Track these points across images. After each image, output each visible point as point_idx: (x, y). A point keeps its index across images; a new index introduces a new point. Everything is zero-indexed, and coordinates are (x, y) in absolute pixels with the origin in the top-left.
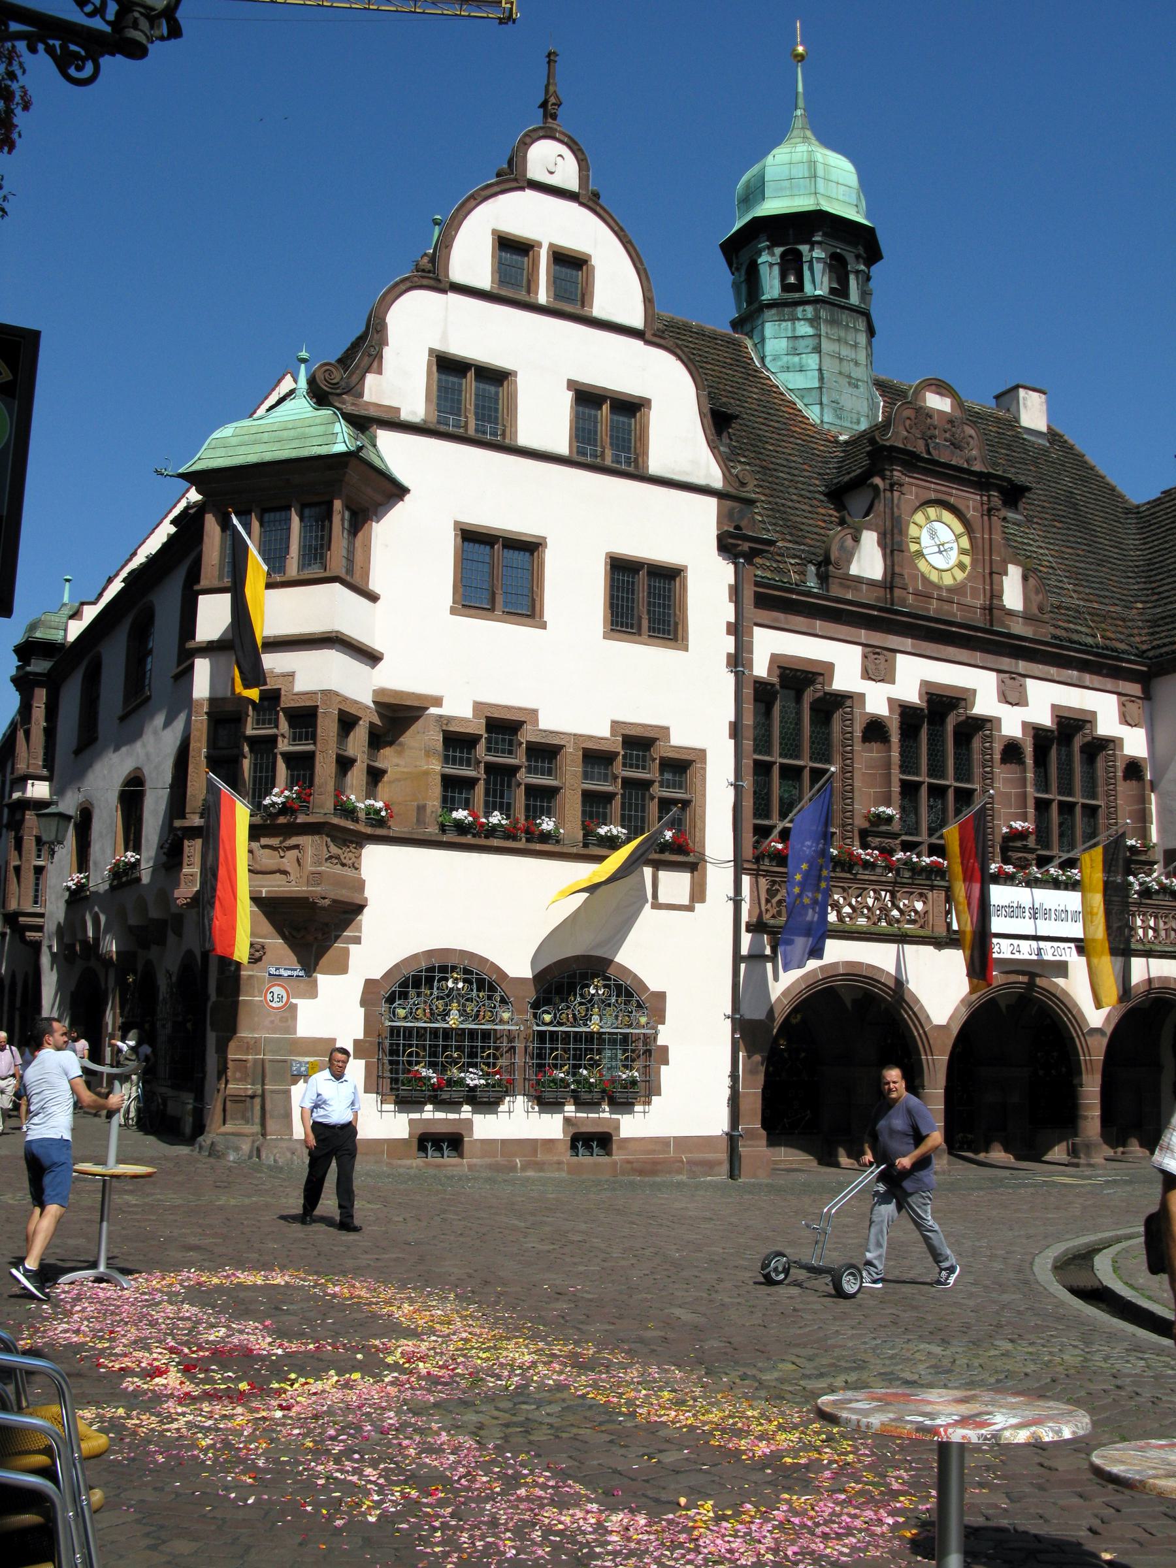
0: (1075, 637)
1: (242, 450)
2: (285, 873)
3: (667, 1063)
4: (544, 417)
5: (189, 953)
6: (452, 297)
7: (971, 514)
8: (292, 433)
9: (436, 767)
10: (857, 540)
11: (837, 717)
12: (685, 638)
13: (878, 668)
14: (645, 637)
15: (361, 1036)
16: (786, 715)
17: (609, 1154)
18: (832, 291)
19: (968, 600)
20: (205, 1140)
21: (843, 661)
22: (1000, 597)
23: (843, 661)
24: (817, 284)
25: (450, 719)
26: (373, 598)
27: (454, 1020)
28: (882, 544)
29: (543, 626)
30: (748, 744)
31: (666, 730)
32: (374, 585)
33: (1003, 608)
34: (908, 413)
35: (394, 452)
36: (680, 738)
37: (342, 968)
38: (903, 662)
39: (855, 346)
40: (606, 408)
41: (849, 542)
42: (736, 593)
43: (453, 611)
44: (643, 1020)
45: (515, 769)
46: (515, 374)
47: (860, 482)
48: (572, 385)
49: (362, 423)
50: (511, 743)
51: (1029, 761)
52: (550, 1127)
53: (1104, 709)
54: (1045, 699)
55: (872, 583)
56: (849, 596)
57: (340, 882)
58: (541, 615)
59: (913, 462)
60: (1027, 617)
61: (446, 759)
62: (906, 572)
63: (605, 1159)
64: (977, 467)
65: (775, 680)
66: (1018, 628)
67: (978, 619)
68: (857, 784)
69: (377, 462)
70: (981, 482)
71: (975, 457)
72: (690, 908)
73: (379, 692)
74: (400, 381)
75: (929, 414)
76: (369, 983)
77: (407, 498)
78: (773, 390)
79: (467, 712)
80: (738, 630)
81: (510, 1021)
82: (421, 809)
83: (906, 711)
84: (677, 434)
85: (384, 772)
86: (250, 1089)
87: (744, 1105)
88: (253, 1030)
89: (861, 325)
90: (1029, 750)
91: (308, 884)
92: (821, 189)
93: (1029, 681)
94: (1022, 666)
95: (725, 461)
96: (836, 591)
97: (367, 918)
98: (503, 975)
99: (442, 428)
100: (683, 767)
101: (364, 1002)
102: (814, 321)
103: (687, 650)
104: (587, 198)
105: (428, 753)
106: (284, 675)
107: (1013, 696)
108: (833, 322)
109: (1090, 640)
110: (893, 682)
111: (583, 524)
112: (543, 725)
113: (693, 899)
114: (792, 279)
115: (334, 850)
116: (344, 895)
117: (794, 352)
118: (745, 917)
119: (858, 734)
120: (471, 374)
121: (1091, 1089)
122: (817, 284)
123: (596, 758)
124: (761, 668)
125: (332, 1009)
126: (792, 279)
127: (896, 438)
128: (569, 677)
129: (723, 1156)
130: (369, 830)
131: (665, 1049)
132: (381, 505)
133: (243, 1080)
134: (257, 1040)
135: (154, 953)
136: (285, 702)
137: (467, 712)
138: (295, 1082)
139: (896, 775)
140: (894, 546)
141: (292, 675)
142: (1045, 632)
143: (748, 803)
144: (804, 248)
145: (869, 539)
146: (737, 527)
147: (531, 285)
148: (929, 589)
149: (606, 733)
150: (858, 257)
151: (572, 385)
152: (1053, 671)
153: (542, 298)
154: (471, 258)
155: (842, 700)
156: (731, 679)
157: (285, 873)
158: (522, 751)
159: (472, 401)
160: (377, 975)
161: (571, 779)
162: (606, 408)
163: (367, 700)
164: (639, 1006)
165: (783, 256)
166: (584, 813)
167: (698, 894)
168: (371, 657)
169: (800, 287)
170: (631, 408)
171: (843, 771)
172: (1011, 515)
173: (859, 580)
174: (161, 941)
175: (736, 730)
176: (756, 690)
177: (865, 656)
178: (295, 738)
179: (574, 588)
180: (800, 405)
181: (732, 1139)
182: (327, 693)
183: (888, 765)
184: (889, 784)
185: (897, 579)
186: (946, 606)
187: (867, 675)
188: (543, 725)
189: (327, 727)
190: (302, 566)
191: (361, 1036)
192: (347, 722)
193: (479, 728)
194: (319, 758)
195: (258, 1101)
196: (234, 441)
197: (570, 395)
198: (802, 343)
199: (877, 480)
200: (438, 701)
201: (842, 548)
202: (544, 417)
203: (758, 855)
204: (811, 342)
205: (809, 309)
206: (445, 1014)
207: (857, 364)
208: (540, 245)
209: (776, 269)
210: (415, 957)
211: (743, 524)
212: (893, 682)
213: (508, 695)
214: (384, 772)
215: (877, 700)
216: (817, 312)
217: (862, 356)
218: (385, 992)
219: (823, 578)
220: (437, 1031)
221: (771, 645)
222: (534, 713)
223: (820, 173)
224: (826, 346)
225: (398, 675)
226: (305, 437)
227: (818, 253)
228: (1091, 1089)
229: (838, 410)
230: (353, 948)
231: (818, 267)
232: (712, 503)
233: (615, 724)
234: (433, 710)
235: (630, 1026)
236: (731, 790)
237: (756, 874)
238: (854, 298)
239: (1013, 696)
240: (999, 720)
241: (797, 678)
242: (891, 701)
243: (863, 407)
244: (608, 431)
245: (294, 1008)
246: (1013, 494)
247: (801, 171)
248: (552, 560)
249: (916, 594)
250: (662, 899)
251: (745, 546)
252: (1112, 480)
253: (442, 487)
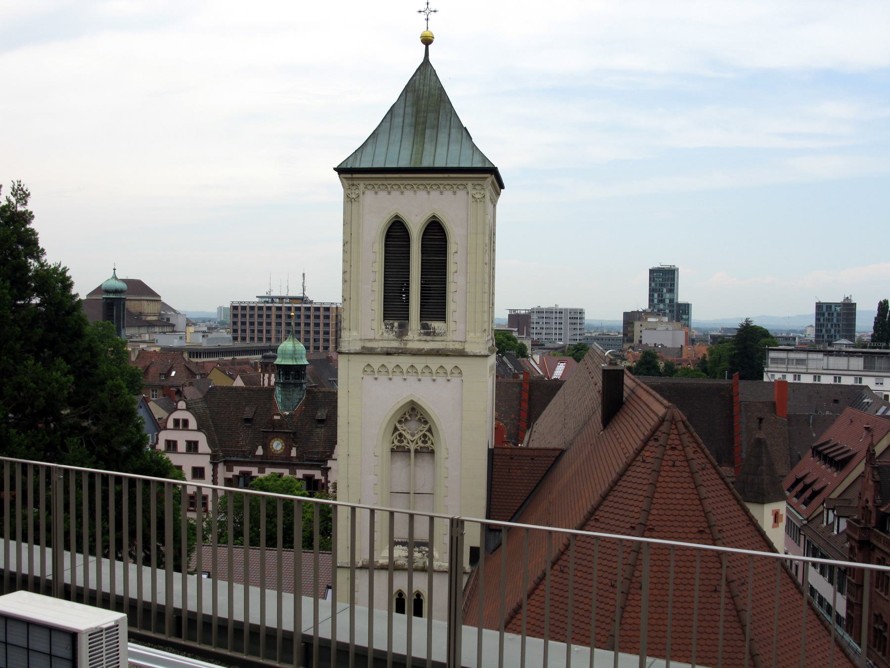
4: (182, 447)
13: (262, 471)
60: (297, 457)
104: (188, 409)
140: (266, 447)
145: (260, 448)
154: (170, 424)
155: (255, 477)
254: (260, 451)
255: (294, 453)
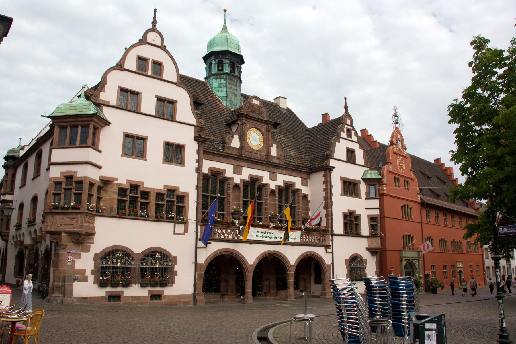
0: (290, 163)
1: (66, 111)
2: (73, 225)
3: (177, 275)
4: (149, 105)
5: (48, 245)
6: (125, 72)
7: (263, 131)
8: (79, 107)
9: (116, 197)
10: (233, 137)
11: (226, 183)
12: (184, 164)
13: (237, 171)
14: (174, 163)
15: (93, 269)
16: (212, 185)
17: (161, 300)
18: (231, 71)
19: (262, 153)
20: (48, 298)
21: (228, 169)
22: (270, 153)
23: (228, 169)
24: (227, 69)
25: (120, 184)
26: (100, 152)
27: (119, 265)
28: (240, 139)
29: (146, 160)
30: (201, 191)
31: (179, 187)
32: (100, 149)
33: (271, 155)
34: (248, 105)
35: (107, 113)
36: (183, 190)
37: (88, 250)
38: (244, 169)
39: (236, 86)
40: (165, 102)
41: (231, 138)
42: (198, 152)
43: (122, 156)
44: (170, 264)
45: (137, 197)
46: (141, 93)
47: (234, 123)
48: (156, 96)
49: (99, 105)
50: (137, 191)
51: (277, 195)
52: (144, 292)
53: (297, 181)
54: (281, 179)
55: (236, 149)
56: (230, 152)
57: (88, 228)
58: (146, 157)
59: (248, 117)
60: (278, 158)
61: (119, 195)
62: (246, 146)
63: (159, 301)
64: (265, 119)
65: (210, 174)
66: (275, 161)
67: (264, 158)
68: (231, 201)
69: (102, 116)
70: (267, 123)
71: (265, 116)
72: (184, 234)
73: (100, 177)
74: (110, 95)
75: (253, 105)
76: (96, 255)
77: (110, 125)
78: (214, 97)
79: (125, 182)
80: (199, 161)
81: (135, 264)
82: (112, 208)
83: (245, 182)
84: (185, 110)
85: (102, 198)
86: (61, 284)
87: (198, 286)
88: (62, 268)
89: (238, 80)
90: (277, 192)
91: (79, 228)
92: (229, 45)
93: (278, 175)
94: (276, 170)
95: (197, 116)
96: (227, 151)
97: (96, 237)
98: (133, 252)
99: (121, 107)
100: (182, 198)
101: (94, 260)
102: (225, 79)
103: (184, 166)
105: (114, 193)
106: (74, 172)
107: (273, 178)
108: (230, 80)
109: (294, 164)
110: (241, 174)
111: (158, 134)
112: (145, 186)
113: (184, 232)
114: (220, 68)
115: (87, 219)
116: (89, 231)
117: (220, 87)
118: (199, 237)
119: (232, 188)
120: (129, 93)
121: (291, 280)
122: (227, 69)
123: (159, 195)
124: (205, 170)
125: (86, 262)
126: (220, 68)
127: (243, 111)
128: (154, 174)
129: (192, 300)
130: (96, 214)
131: (177, 271)
132: (103, 127)
133: (59, 281)
134: (64, 270)
135: (39, 245)
136: (74, 179)
137: (125, 182)
138: (74, 282)
139: (242, 199)
140: (243, 138)
141: (77, 172)
142: (282, 162)
143: (200, 207)
144: (224, 60)
145: (236, 137)
146: (199, 135)
147: (146, 70)
148: (252, 151)
149: (162, 188)
150: (238, 63)
151: (157, 96)
152: (284, 171)
153: (149, 73)
156: (196, 174)
157: (73, 225)
158: (139, 193)
159: (129, 99)
160: (98, 252)
161: (152, 201)
162: (165, 102)
163: (97, 179)
164: (170, 260)
165: (218, 61)
166: (156, 209)
167: (186, 230)
168: (100, 167)
169: (222, 70)
170: (173, 103)
171: (228, 197)
172: (275, 130)
173: (233, 148)
174: (41, 242)
175: (197, 188)
176: (203, 176)
177: (234, 168)
178: (76, 189)
179: (155, 150)
180: (221, 101)
181: (194, 295)
182: (86, 178)
183: (239, 196)
184: (239, 201)
185: (243, 148)
186: (256, 155)
187: (234, 173)
188: (145, 186)
189: (86, 187)
190: (81, 143)
191: (93, 269)
192: (91, 185)
193: (128, 187)
194: (83, 194)
195: (63, 287)
196: (63, 108)
197: (156, 99)
198: (222, 85)
199: (239, 122)
200: (117, 180)
201: (229, 139)
202: (149, 105)
203: (203, 220)
204: (225, 85)
205: (225, 76)
206: (117, 263)
207: (236, 90)
208: (149, 59)
209: (216, 65)
210: (109, 247)
211: (201, 133)
212: (241, 174)
213: (136, 178)
214: (102, 198)
215: (237, 179)
216: (226, 76)
217: (238, 89)
218: (100, 257)
219: (223, 147)
220: (115, 267)
221: (208, 165)
222: (143, 183)
223: (229, 41)
224: (228, 85)
225: (107, 172)
226: (82, 109)
227: (227, 62)
228: (291, 280)
229: (231, 102)
230: (91, 245)
231: (227, 65)
232: (193, 128)
233: (165, 186)
234: (116, 182)
235: (167, 265)
236: (196, 203)
237: (201, 225)
238: (236, 73)
239: (273, 178)
240: (269, 184)
241: (216, 174)
242: (240, 179)
243: (238, 102)
244: (166, 109)
245: (74, 261)
246: (276, 125)
247: (224, 40)
248: (149, 143)
249: (248, 152)
250: (176, 232)
251: (201, 140)
252: (303, 121)
253: (120, 123)
254: (235, 143)
255: (274, 152)
